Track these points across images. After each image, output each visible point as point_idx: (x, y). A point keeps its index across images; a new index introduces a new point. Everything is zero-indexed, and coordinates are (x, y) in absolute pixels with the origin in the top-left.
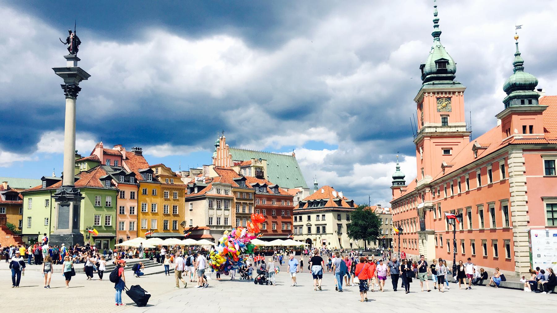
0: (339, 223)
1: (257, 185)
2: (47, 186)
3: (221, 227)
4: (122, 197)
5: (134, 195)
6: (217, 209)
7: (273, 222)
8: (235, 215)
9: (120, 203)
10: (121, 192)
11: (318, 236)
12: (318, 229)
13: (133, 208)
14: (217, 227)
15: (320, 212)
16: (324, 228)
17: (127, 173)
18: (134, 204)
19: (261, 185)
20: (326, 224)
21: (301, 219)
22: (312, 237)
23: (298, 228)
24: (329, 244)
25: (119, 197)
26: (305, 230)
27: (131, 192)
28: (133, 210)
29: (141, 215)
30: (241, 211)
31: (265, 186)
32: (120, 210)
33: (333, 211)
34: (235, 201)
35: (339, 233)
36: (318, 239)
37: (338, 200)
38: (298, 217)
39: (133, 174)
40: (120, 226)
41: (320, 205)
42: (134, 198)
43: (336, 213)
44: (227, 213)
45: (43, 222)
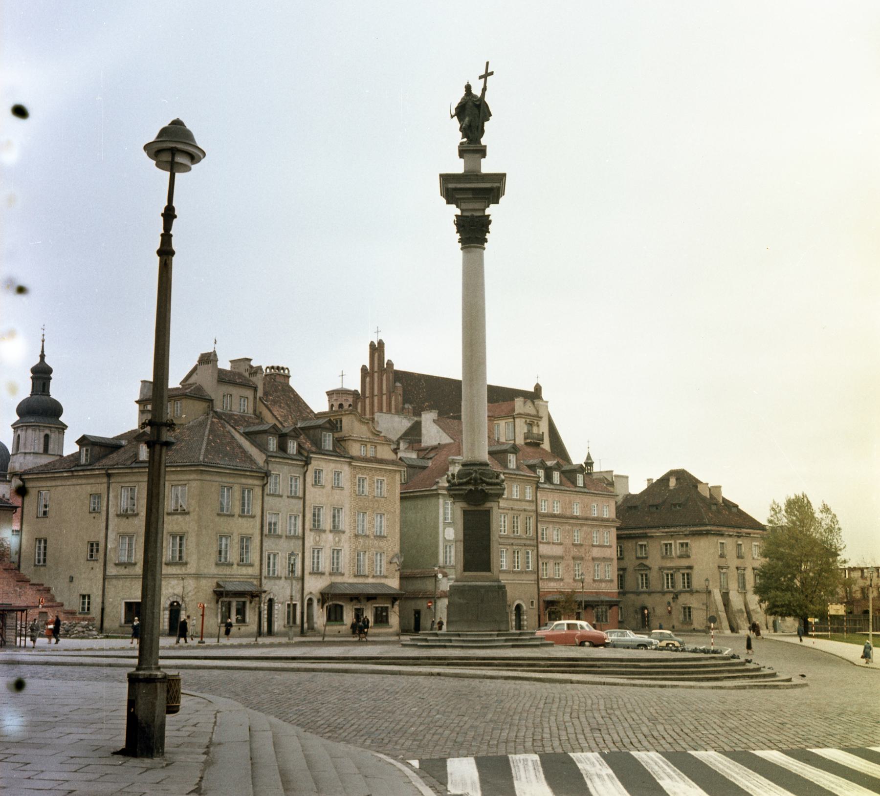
0: (722, 562)
20: (690, 568)
31: (558, 467)
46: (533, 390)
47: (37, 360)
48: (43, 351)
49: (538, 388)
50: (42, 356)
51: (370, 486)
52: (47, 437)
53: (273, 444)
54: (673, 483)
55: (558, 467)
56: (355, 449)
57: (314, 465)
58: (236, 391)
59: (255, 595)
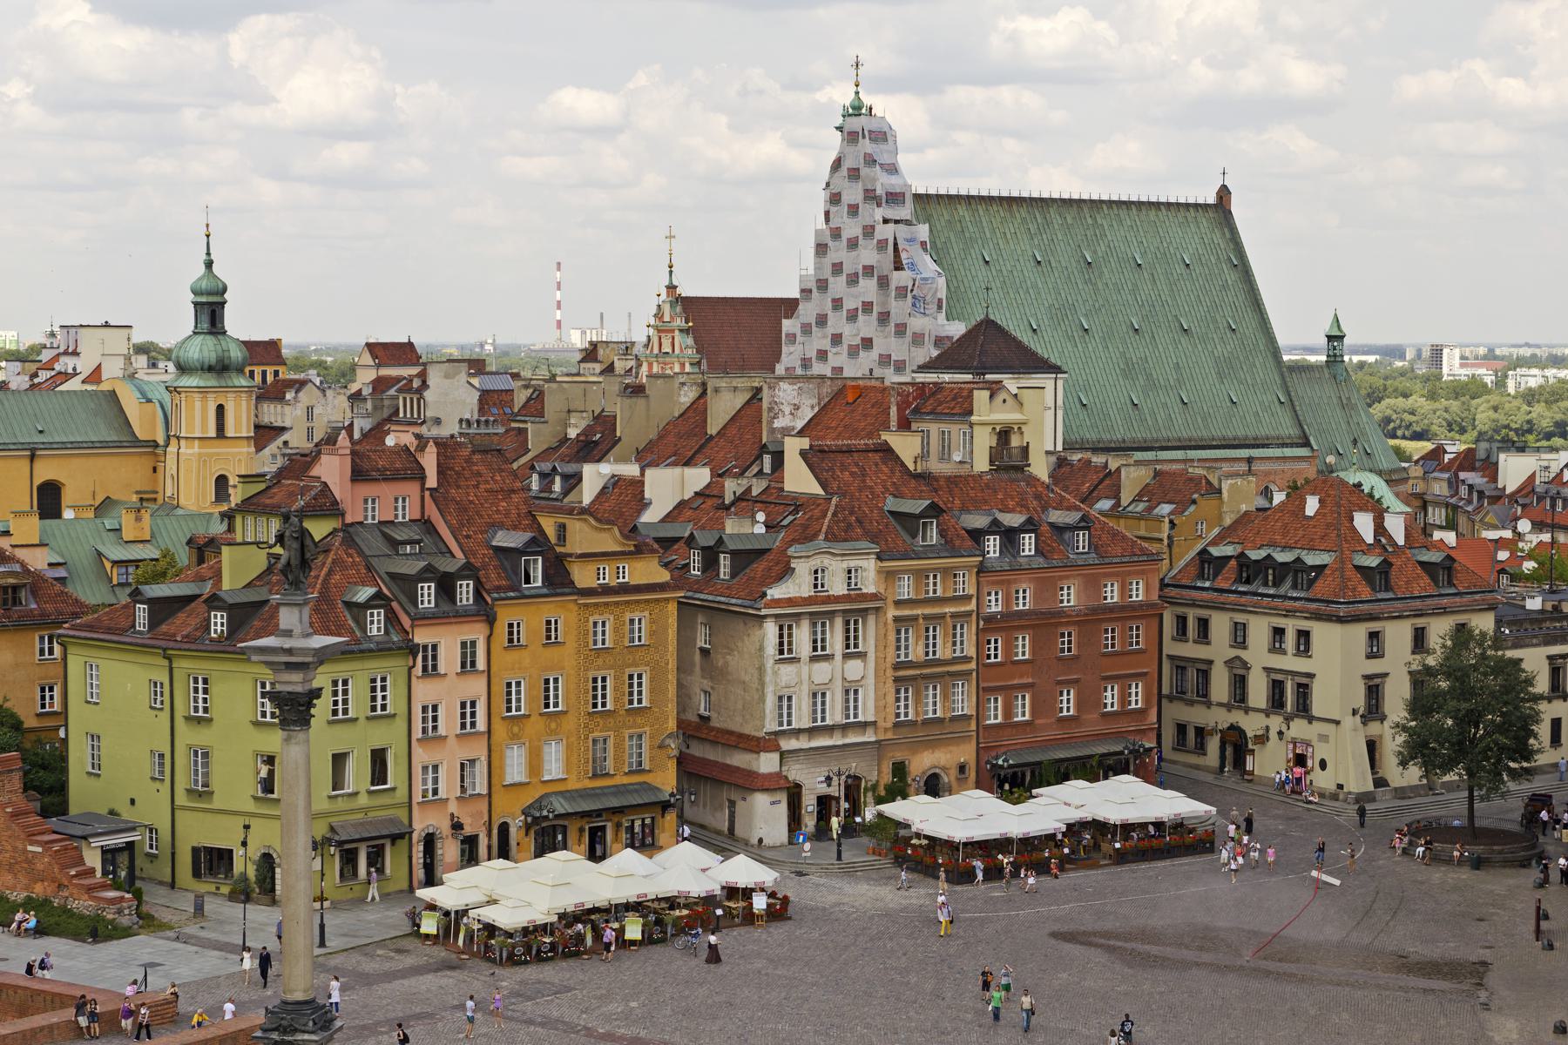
0: (1375, 667)
1: (995, 527)
2: (154, 623)
3: (830, 730)
4: (431, 671)
5: (474, 654)
6: (814, 659)
7: (1059, 683)
8: (890, 673)
9: (424, 692)
10: (425, 648)
11: (1276, 722)
12: (1277, 688)
13: (473, 704)
14: (812, 732)
15: (1289, 613)
16: (1303, 691)
17: (449, 566)
18: (475, 687)
19: (1013, 520)
20: (1311, 676)
21: (1204, 624)
22: (1251, 725)
23: (1191, 674)
24: (1323, 764)
25: (418, 670)
26: (1220, 687)
27: (464, 644)
28: (473, 714)
29: (500, 730)
30: (916, 652)
31: (1030, 526)
32: (424, 720)
33: (1341, 620)
34: (892, 612)
35: (1373, 709)
36: (1273, 734)
37: (1372, 561)
38: (1192, 615)
39: (469, 571)
40: (425, 782)
41: (1288, 583)
42: (473, 664)
43: (1360, 631)
44: (854, 668)
45: (147, 767)
46: (1212, 200)
47: (202, 269)
48: (208, 254)
49: (1224, 193)
50: (209, 264)
51: (616, 630)
52: (220, 409)
53: (427, 594)
54: (1312, 505)
55: (1030, 526)
56: (583, 576)
57: (506, 615)
58: (387, 491)
59: (400, 836)
